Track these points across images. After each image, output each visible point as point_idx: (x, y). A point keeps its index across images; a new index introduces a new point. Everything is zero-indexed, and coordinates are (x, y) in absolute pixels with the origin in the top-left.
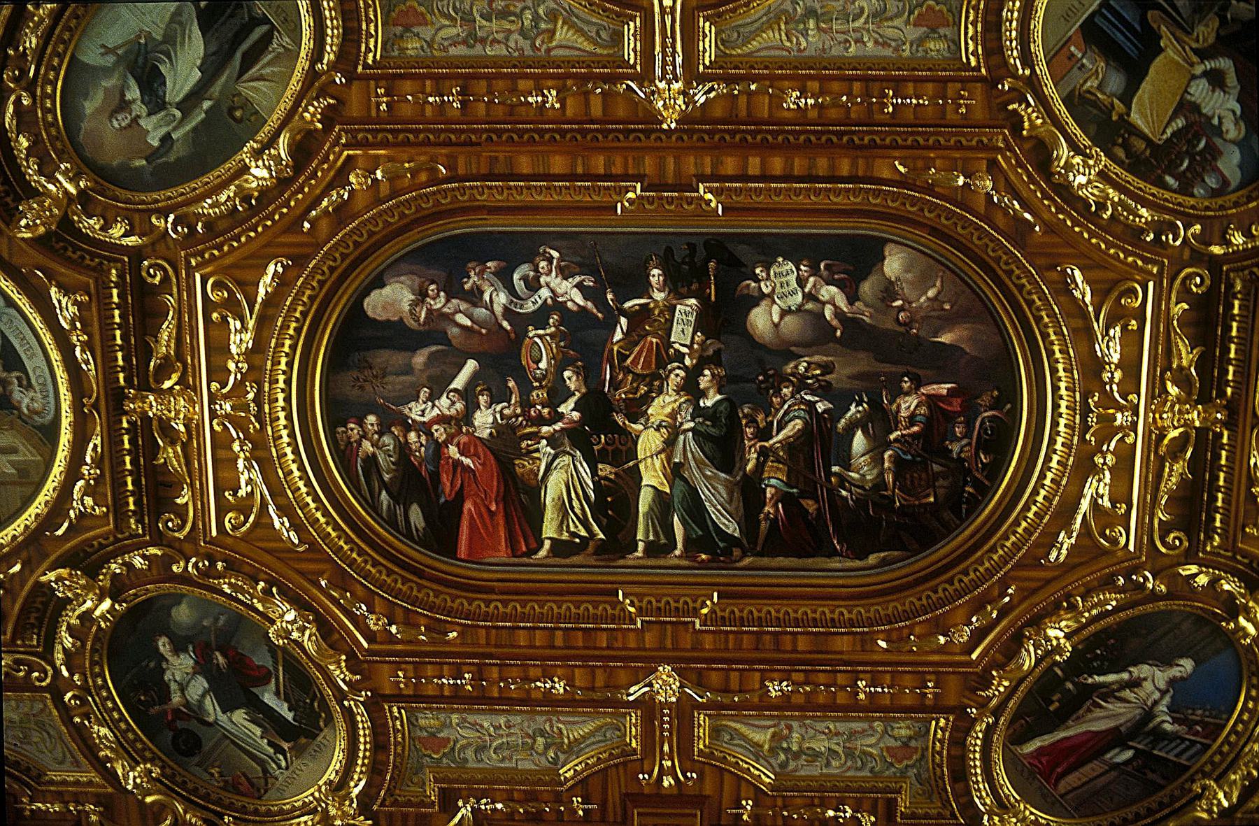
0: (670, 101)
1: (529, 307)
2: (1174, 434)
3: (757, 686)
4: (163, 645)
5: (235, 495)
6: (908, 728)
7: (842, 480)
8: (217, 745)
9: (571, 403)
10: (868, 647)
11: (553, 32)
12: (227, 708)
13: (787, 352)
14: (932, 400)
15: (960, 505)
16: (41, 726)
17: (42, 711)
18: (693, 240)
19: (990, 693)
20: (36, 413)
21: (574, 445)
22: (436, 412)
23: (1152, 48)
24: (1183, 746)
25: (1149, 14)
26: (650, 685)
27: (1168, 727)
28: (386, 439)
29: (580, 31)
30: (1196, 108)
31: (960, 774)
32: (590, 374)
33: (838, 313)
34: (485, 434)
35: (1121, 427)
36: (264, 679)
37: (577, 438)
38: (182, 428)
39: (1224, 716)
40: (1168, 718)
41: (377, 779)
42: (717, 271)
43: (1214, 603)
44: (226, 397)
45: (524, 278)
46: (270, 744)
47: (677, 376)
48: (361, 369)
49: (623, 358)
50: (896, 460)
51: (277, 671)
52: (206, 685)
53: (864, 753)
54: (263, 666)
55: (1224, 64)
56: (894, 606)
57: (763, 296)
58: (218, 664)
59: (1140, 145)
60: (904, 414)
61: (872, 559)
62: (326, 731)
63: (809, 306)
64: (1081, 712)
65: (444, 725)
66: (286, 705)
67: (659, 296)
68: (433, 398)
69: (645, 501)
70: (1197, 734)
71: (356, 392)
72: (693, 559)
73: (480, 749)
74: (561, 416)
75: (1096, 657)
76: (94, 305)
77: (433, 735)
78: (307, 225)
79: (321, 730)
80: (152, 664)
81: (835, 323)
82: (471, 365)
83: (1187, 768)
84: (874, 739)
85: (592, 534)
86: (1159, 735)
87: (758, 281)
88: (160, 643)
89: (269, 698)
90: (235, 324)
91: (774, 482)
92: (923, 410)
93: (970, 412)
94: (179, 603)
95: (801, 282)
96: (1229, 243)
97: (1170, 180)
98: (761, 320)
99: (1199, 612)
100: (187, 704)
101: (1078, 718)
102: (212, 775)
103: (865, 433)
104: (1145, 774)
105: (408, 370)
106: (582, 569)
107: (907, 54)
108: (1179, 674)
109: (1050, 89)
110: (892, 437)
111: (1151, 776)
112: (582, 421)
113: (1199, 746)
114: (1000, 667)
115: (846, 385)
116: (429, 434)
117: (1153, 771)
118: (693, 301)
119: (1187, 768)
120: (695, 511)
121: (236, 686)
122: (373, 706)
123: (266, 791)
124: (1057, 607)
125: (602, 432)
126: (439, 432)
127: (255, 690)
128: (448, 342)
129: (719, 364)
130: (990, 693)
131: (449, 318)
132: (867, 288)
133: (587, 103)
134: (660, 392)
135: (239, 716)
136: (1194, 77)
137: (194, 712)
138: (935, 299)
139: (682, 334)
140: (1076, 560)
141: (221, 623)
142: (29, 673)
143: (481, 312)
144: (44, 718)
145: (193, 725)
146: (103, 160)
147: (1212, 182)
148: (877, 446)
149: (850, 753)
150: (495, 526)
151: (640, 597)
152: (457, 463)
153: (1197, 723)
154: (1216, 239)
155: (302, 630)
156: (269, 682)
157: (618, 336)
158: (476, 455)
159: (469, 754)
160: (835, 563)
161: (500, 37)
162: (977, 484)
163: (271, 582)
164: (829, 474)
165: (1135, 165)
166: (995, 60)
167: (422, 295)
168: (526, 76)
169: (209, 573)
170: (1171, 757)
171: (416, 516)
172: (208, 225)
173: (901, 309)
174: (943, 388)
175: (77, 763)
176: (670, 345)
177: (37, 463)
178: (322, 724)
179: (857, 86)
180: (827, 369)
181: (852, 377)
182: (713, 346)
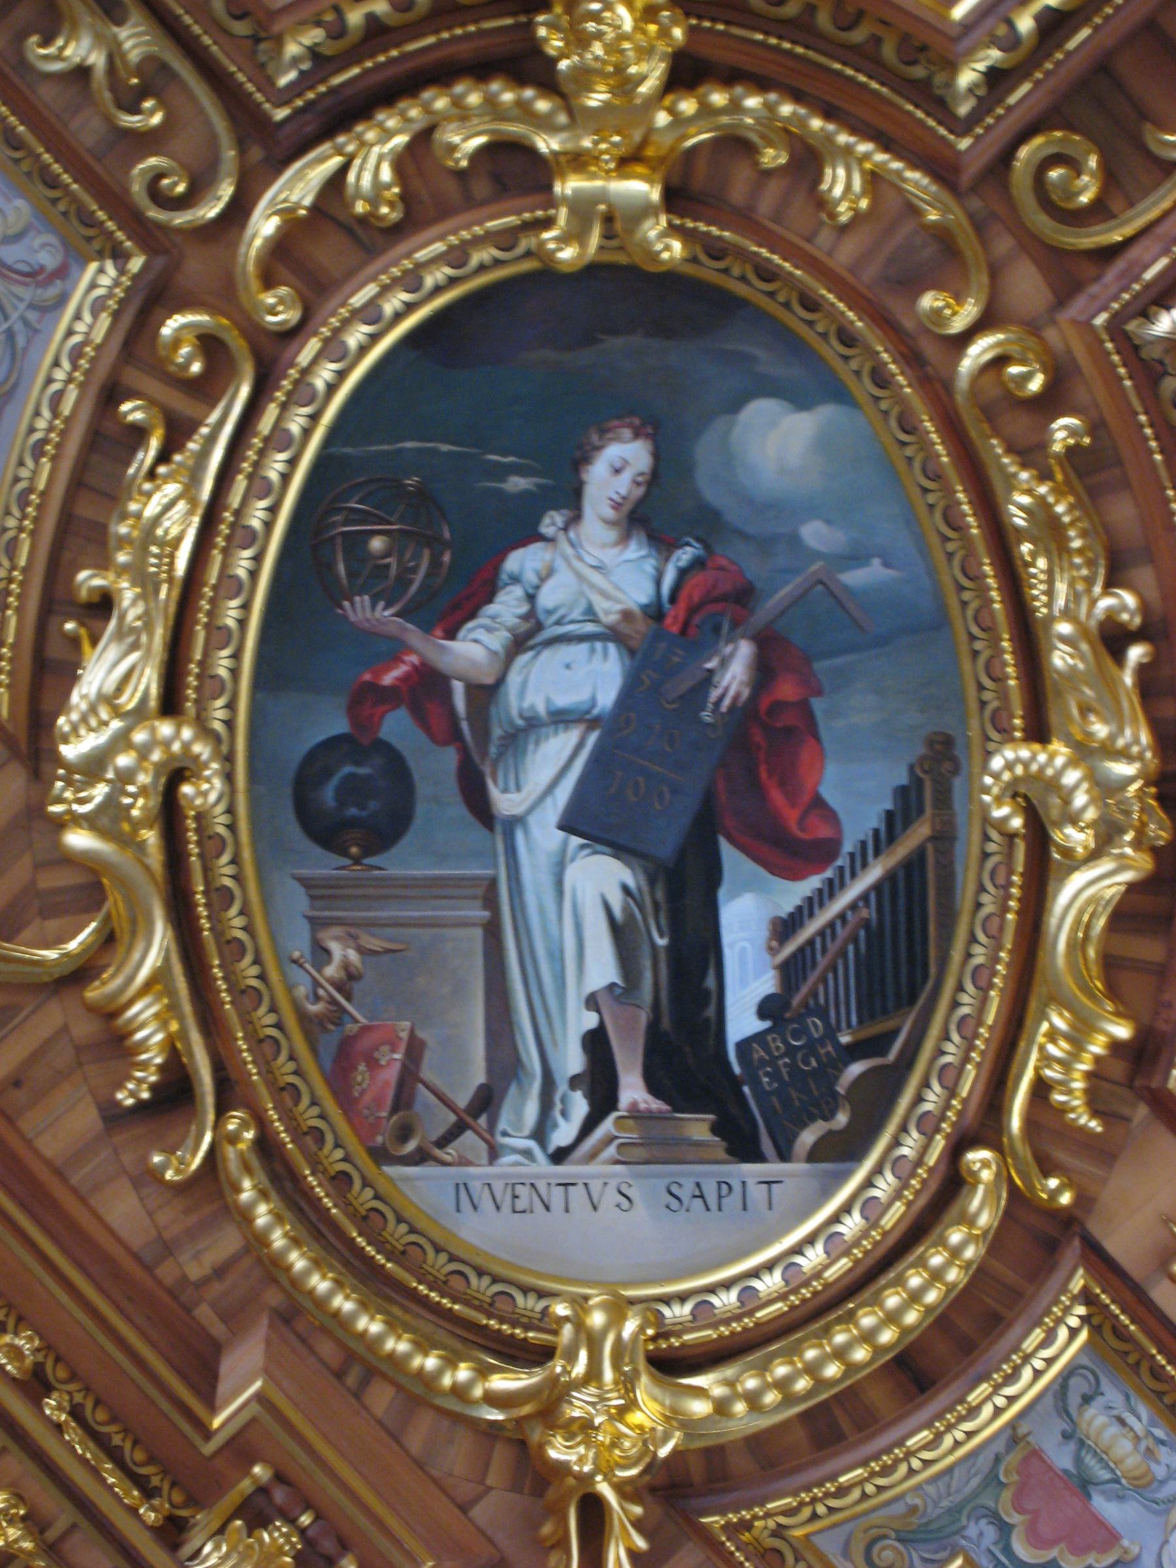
4: (617, 466)
12: (588, 821)
17: (34, 275)
36: (788, 853)
51: (859, 861)
52: (607, 698)
54: (831, 816)
58: (708, 679)
62: (797, 1167)
66: (767, 984)
79: (784, 1155)
80: (517, 484)
88: (613, 452)
89: (746, 915)
94: (801, 402)
100: (485, 694)
102: (321, 954)
121: (695, 789)
122: (1037, 1241)
123: (421, 1157)
127: (729, 854)
135: (602, 880)
137: (482, 733)
141: (855, 578)
145: (434, 769)
155: (1107, 835)
156: (795, 875)
178: (808, 1137)
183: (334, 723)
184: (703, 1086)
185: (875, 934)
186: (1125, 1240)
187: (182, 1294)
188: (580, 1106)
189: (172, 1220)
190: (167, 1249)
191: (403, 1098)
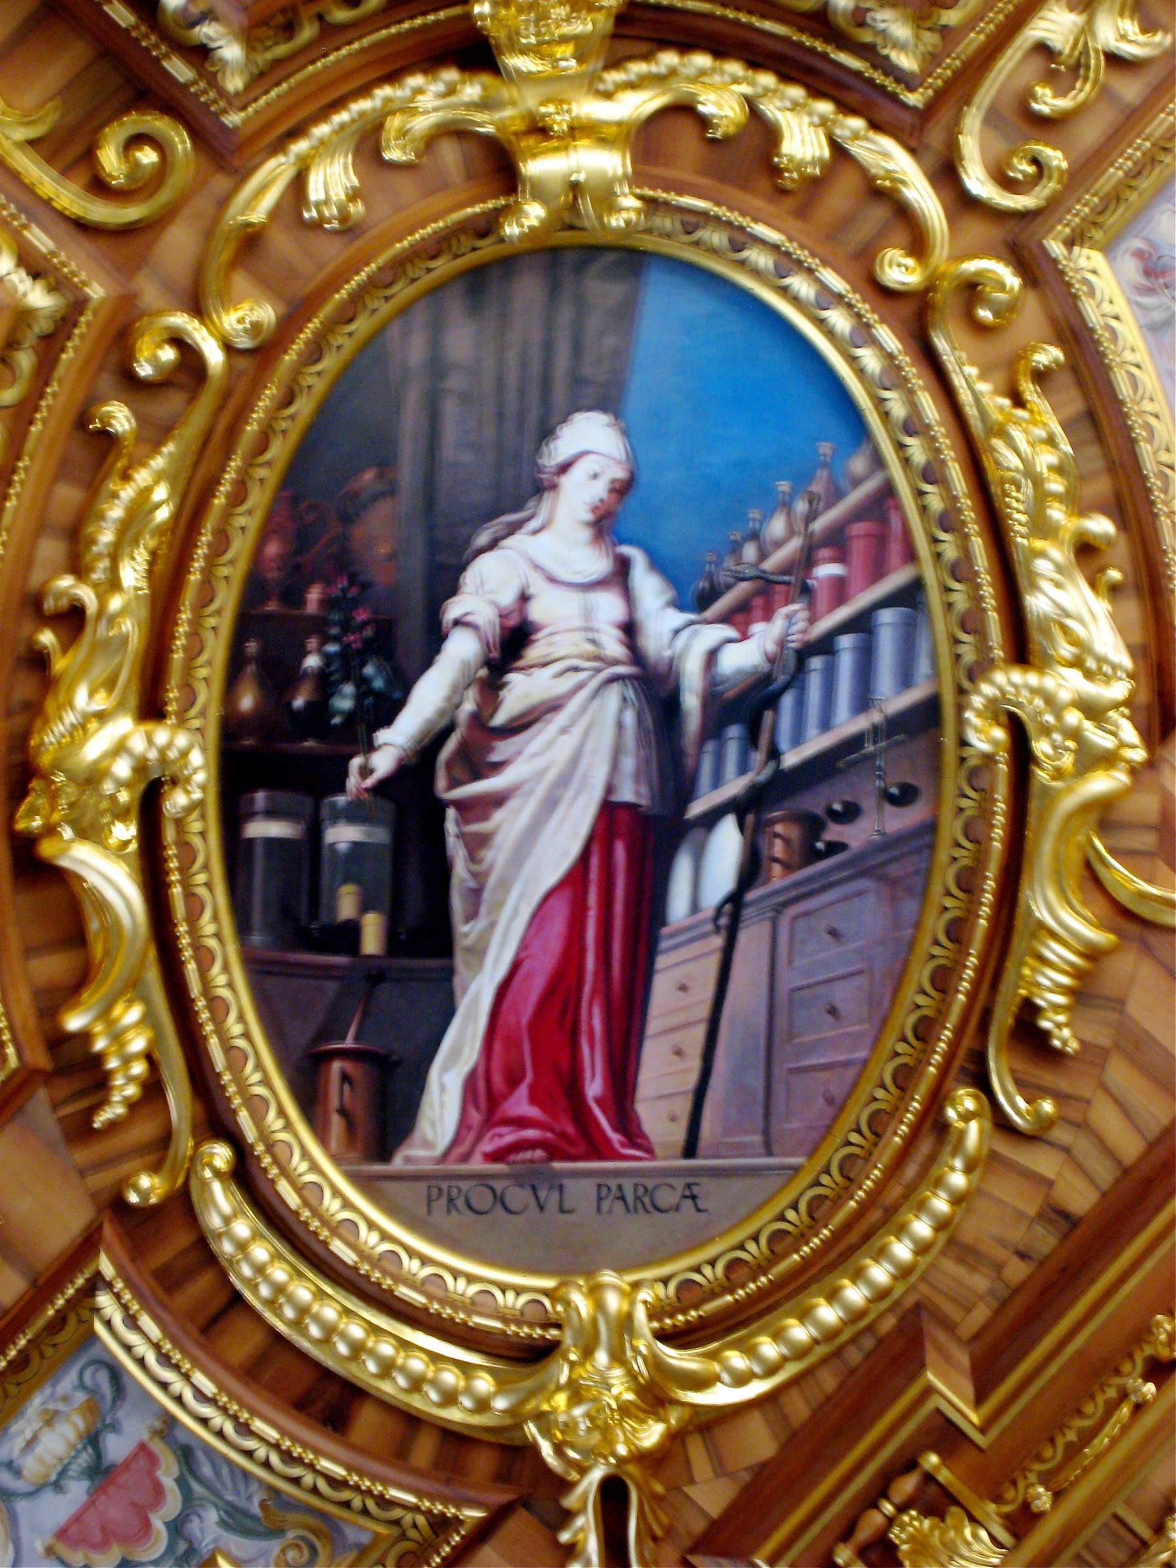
6: (51, 1418)
24: (846, 662)
27: (744, 656)
31: (328, 1399)
39: (859, 464)
43: (439, 201)
64: (460, 870)
70: (840, 591)
75: (325, 683)
83: (926, 718)
86: (747, 707)
99: (443, 266)
101: (476, 894)
104: (835, 848)
108: (599, 490)
111: (857, 835)
113: (887, 616)
117: (850, 813)
153: (807, 559)
170: (848, 724)
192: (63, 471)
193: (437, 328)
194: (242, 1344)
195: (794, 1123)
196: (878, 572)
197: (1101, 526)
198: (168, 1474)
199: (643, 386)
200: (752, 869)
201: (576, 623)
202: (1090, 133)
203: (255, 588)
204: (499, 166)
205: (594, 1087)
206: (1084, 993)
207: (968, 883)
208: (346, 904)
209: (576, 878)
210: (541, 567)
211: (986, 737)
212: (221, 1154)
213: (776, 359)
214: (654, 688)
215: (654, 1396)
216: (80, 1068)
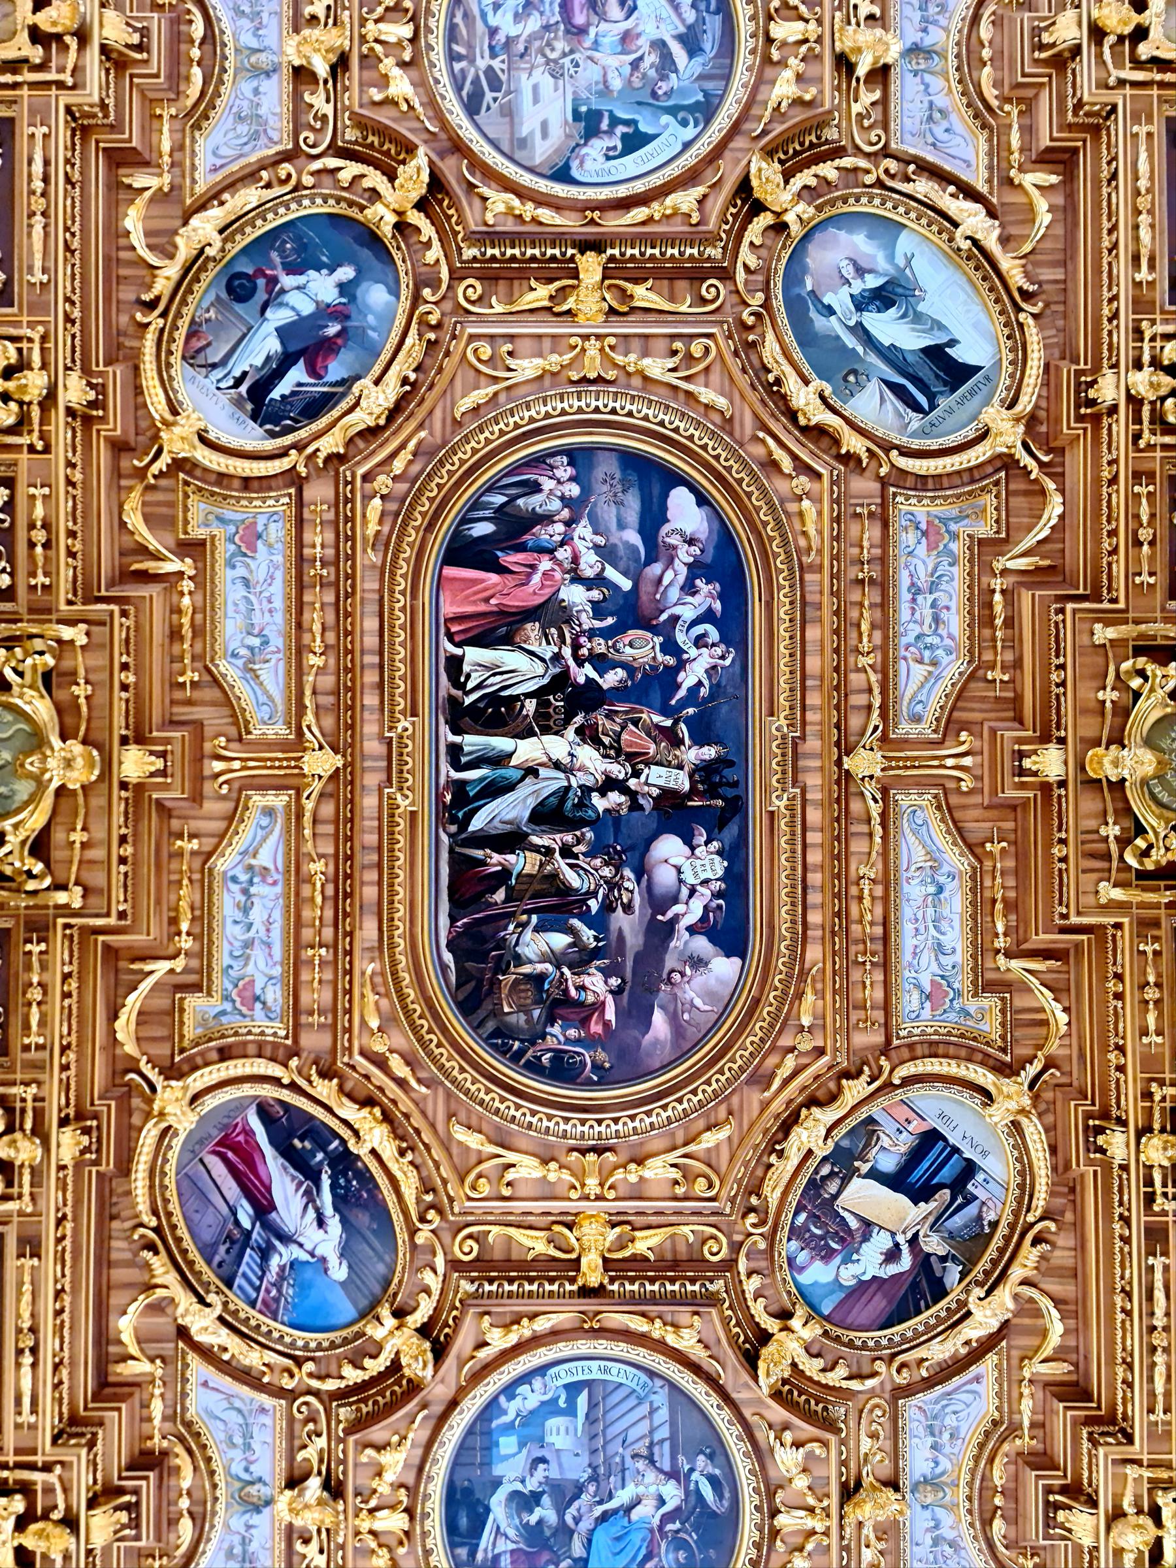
0: (865, 763)
1: (680, 637)
2: (571, 1237)
3: (321, 850)
4: (346, 273)
5: (510, 354)
7: (524, 925)
8: (240, 318)
9: (593, 675)
10: (367, 955)
11: (920, 661)
12: (283, 332)
13: (641, 871)
14: (600, 1006)
15: (500, 1038)
16: (255, 136)
18: (742, 785)
19: (315, 1078)
20: (582, 163)
21: (555, 678)
22: (583, 550)
23: (919, 1195)
25: (947, 1191)
26: (321, 748)
27: (275, 1262)
28: (556, 505)
29: (923, 685)
30: (866, 1238)
31: (225, 1054)
32: (620, 692)
33: (676, 919)
34: (562, 595)
35: (583, 1185)
36: (313, 371)
37: (561, 681)
38: (565, 307)
40: (285, 1260)
41: (213, 478)
42: (715, 806)
44: (602, 350)
45: (705, 635)
46: (245, 374)
47: (618, 771)
48: (622, 481)
49: (636, 722)
50: (540, 978)
52: (305, 313)
53: (248, 958)
55: (906, 1261)
56: (406, 978)
57: (693, 849)
59: (833, 1187)
60: (587, 980)
61: (448, 957)
63: (685, 892)
65: (270, 546)
67: (693, 755)
68: (596, 547)
69: (502, 743)
70: (268, 1291)
71: (601, 476)
72: (446, 788)
73: (246, 582)
74: (580, 663)
75: (348, 1181)
76: (686, 229)
77: (259, 536)
78: (761, 434)
81: (670, 914)
82: (626, 584)
83: (229, 1284)
84: (265, 970)
85: (467, 693)
86: (265, 1253)
87: (706, 843)
89: (297, 374)
90: (671, 363)
91: (522, 863)
92: (591, 999)
93: (590, 1042)
94: (390, 292)
95: (705, 882)
96: (749, 1275)
97: (802, 1217)
98: (669, 847)
100: (283, 291)
103: (571, 945)
105: (622, 526)
106: (433, 686)
107: (907, 974)
109: (883, 1101)
110: (565, 970)
111: (222, 1249)
112: (576, 685)
114: (341, 1088)
115: (614, 927)
116: (562, 544)
118: (687, 787)
119: (230, 1285)
120: (495, 790)
121: (307, 345)
122: (292, 478)
124: (402, 1138)
125: (568, 701)
126: (563, 554)
127: (301, 362)
128: (648, 563)
129: (631, 809)
130: (315, 1078)
131: (670, 562)
132: (701, 944)
133: (860, 692)
134: (605, 756)
135: (274, 345)
136: (893, 1234)
138: (692, 1005)
139: (657, 777)
140: (455, 1151)
142: (312, 129)
143: (674, 594)
144: (263, 140)
145: (261, 296)
146: (812, 248)
147: (802, 1257)
148: (557, 959)
149: (248, 944)
150: (474, 603)
151: (412, 737)
152: (533, 567)
153: (279, 1291)
154: (754, 1265)
157: (657, 719)
158: (543, 586)
159: (241, 571)
160: (444, 921)
161: (917, 615)
162: (521, 1053)
163: (414, 385)
164: (529, 912)
165: (815, 1186)
166: (905, 1053)
167: (691, 542)
168: (886, 638)
169: (424, 323)
170: (243, 1268)
171: (482, 529)
172: (753, 344)
173: (683, 974)
174: (610, 1014)
175: (215, 170)
176: (648, 764)
177: (532, 158)
179: (879, 930)
180: (628, 908)
181: (620, 930)
182: (647, 804)
183: (250, 271)
184: (257, 398)
185: (315, 400)
186: (308, 494)
187: (120, 346)
188: (231, 382)
189: (131, 330)
190: (125, 335)
191: (199, 351)
192: (429, 1177)
193: (387, 1266)
194: (252, 1049)
195: (185, 1183)
196: (264, 1302)
197: (226, 1357)
198: (244, 1010)
199: (340, 1292)
200: (237, 1223)
201: (311, 1236)
202: (297, 1426)
203: (377, 1186)
204: (400, 1314)
205: (230, 1154)
206: (147, 1266)
207: (191, 1264)
208: (308, 1145)
209: (269, 1189)
210: (327, 1242)
211: (211, 1298)
212: (286, 1081)
213: (319, 1322)
214: (286, 1239)
215: (162, 1115)
216: (324, 1075)
